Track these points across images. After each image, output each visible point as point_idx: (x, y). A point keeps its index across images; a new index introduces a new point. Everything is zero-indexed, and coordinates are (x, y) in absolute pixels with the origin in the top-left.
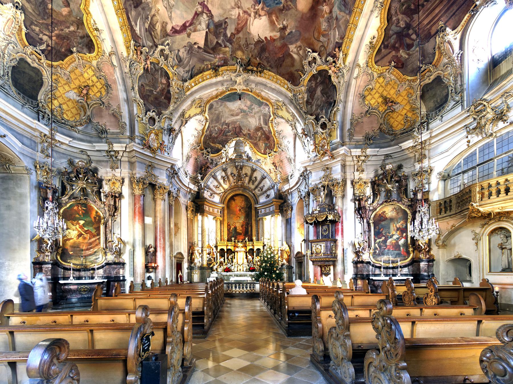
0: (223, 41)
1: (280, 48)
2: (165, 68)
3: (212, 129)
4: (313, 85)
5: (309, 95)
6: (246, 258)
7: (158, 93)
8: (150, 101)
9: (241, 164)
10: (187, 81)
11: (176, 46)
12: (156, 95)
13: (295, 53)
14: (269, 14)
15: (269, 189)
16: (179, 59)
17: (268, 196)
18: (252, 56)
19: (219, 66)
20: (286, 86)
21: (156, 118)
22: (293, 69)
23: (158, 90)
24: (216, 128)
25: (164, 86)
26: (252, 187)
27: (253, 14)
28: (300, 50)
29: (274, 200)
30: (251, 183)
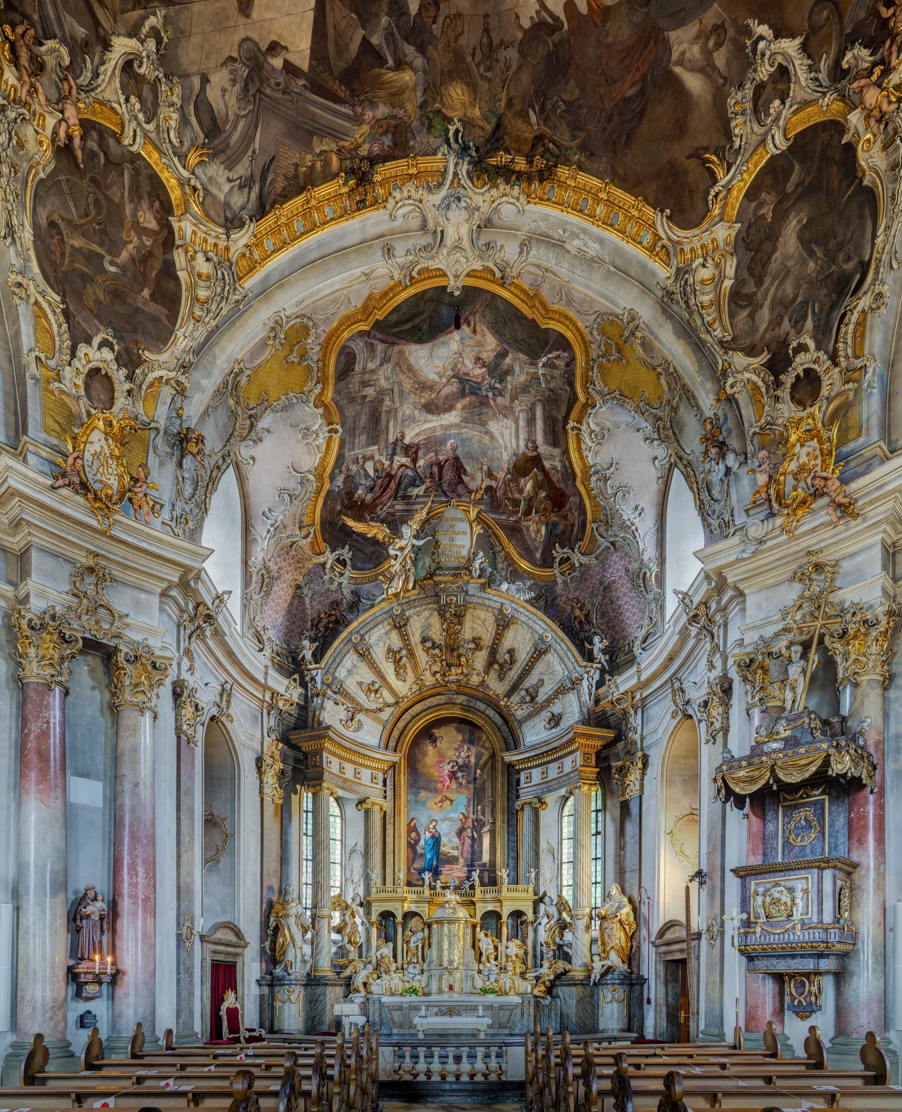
0: (389, 37)
2: (153, 158)
4: (767, 211)
5: (747, 260)
6: (474, 947)
7: (123, 268)
8: (91, 304)
10: (242, 225)
11: (193, 55)
13: (692, 70)
15: (561, 691)
16: (207, 122)
17: (555, 720)
18: (510, 103)
19: (373, 161)
20: (648, 239)
21: (119, 375)
22: (679, 152)
23: (124, 255)
24: (370, 467)
26: (497, 687)
28: (718, 45)
29: (582, 729)
30: (493, 675)
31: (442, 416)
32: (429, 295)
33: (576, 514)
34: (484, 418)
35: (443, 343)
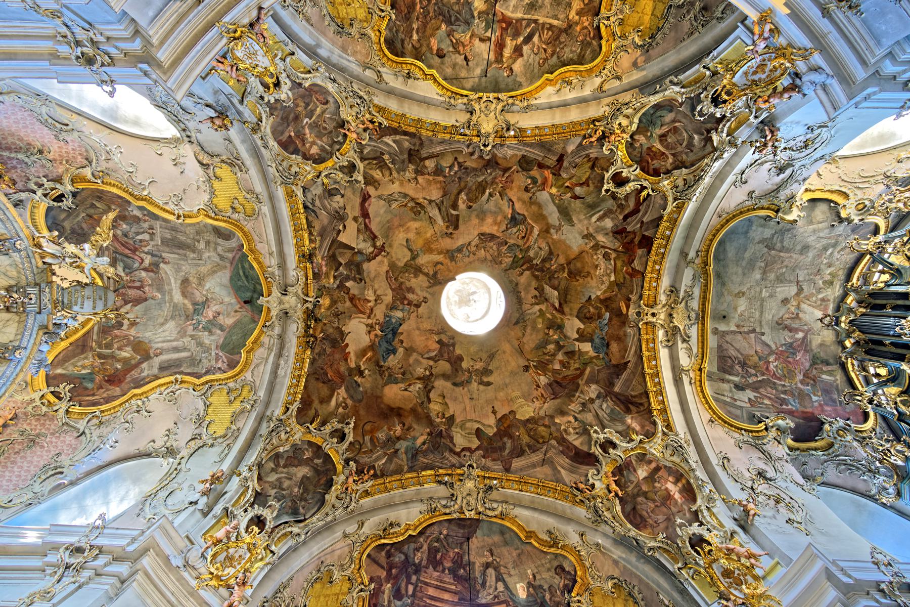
1: (339, 372)
3: (146, 225)
7: (303, 128)
9: (32, 308)
12: (302, 122)
14: (372, 347)
23: (307, 131)
25: (308, 145)
27: (370, 321)
31: (179, 291)
32: (258, 287)
33: (105, 395)
34: (177, 318)
35: (229, 293)
